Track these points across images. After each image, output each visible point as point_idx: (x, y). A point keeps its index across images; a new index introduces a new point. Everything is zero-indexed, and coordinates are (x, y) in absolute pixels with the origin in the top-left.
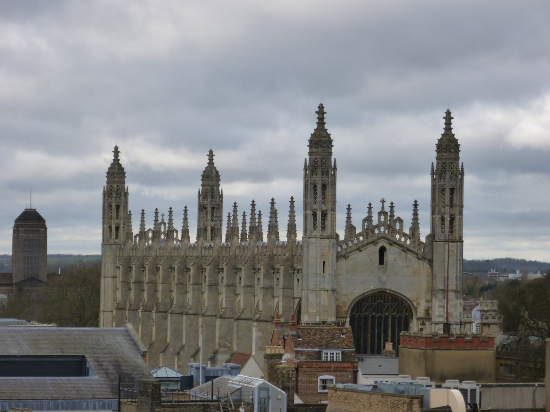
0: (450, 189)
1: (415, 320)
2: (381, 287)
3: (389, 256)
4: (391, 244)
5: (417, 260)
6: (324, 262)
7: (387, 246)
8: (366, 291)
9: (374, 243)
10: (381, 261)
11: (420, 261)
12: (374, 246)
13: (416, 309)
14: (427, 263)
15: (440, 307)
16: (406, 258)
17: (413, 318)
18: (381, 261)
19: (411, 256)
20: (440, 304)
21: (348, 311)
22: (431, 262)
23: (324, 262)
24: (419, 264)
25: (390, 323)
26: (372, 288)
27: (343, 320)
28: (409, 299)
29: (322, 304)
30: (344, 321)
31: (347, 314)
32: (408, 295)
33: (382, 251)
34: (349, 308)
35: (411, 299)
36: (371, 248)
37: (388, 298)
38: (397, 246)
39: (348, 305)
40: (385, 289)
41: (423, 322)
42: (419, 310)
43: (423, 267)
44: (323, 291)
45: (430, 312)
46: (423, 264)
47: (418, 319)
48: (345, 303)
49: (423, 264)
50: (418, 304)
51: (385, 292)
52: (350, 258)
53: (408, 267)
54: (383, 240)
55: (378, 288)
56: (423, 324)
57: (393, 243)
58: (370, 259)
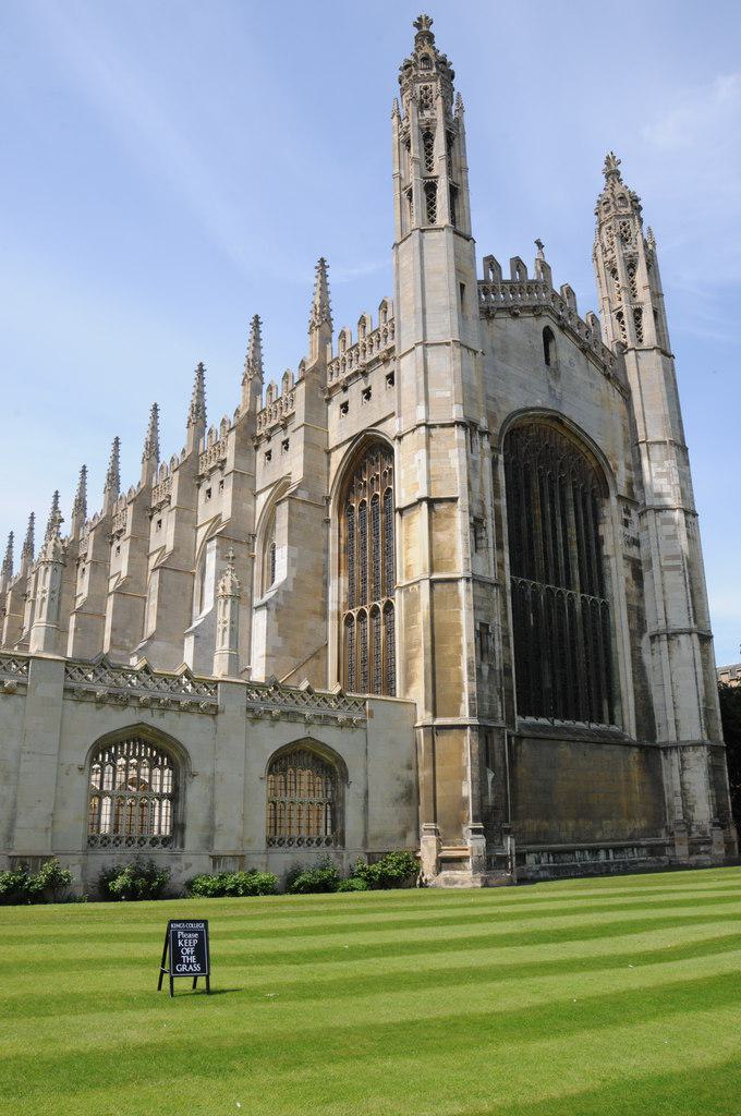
1: (613, 499)
2: (555, 408)
4: (562, 328)
6: (462, 287)
8: (530, 405)
9: (536, 311)
10: (547, 361)
11: (609, 384)
13: (614, 475)
15: (660, 475)
17: (607, 497)
18: (547, 361)
20: (659, 470)
25: (570, 495)
26: (539, 403)
33: (548, 335)
34: (502, 430)
45: (635, 488)
47: (619, 497)
50: (616, 468)
51: (561, 422)
56: (627, 512)
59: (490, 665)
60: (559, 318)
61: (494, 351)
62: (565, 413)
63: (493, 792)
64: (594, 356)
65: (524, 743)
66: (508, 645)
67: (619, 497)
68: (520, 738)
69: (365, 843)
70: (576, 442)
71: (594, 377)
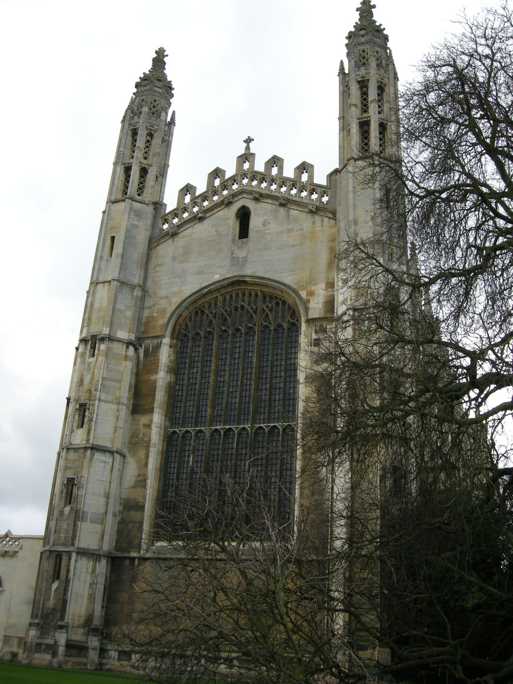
0: (359, 82)
2: (235, 274)
3: (255, 222)
4: (256, 199)
5: (309, 216)
6: (113, 238)
7: (251, 205)
9: (227, 203)
12: (226, 209)
13: (306, 304)
14: (330, 218)
16: (288, 216)
19: (297, 212)
21: (168, 323)
22: (334, 213)
23: (113, 238)
24: (314, 223)
26: (217, 277)
27: (156, 342)
28: (289, 287)
29: (96, 306)
30: (158, 343)
31: (166, 330)
32: (288, 279)
34: (170, 319)
35: (295, 286)
36: (222, 212)
37: (257, 295)
38: (270, 201)
39: (168, 315)
40: (241, 276)
41: (322, 326)
42: (311, 305)
43: (322, 226)
44: (102, 284)
46: (322, 221)
47: (309, 321)
48: (164, 311)
49: (322, 221)
50: (311, 294)
51: (244, 282)
52: (180, 235)
53: (289, 231)
54: (244, 196)
55: (229, 275)
57: (259, 197)
58: (216, 231)
59: (71, 507)
60: (250, 193)
61: (174, 259)
62: (249, 271)
63: (55, 598)
64: (299, 204)
65: (148, 563)
66: (144, 487)
67: (309, 321)
68: (144, 559)
69: (5, 630)
70: (271, 290)
71: (296, 220)
